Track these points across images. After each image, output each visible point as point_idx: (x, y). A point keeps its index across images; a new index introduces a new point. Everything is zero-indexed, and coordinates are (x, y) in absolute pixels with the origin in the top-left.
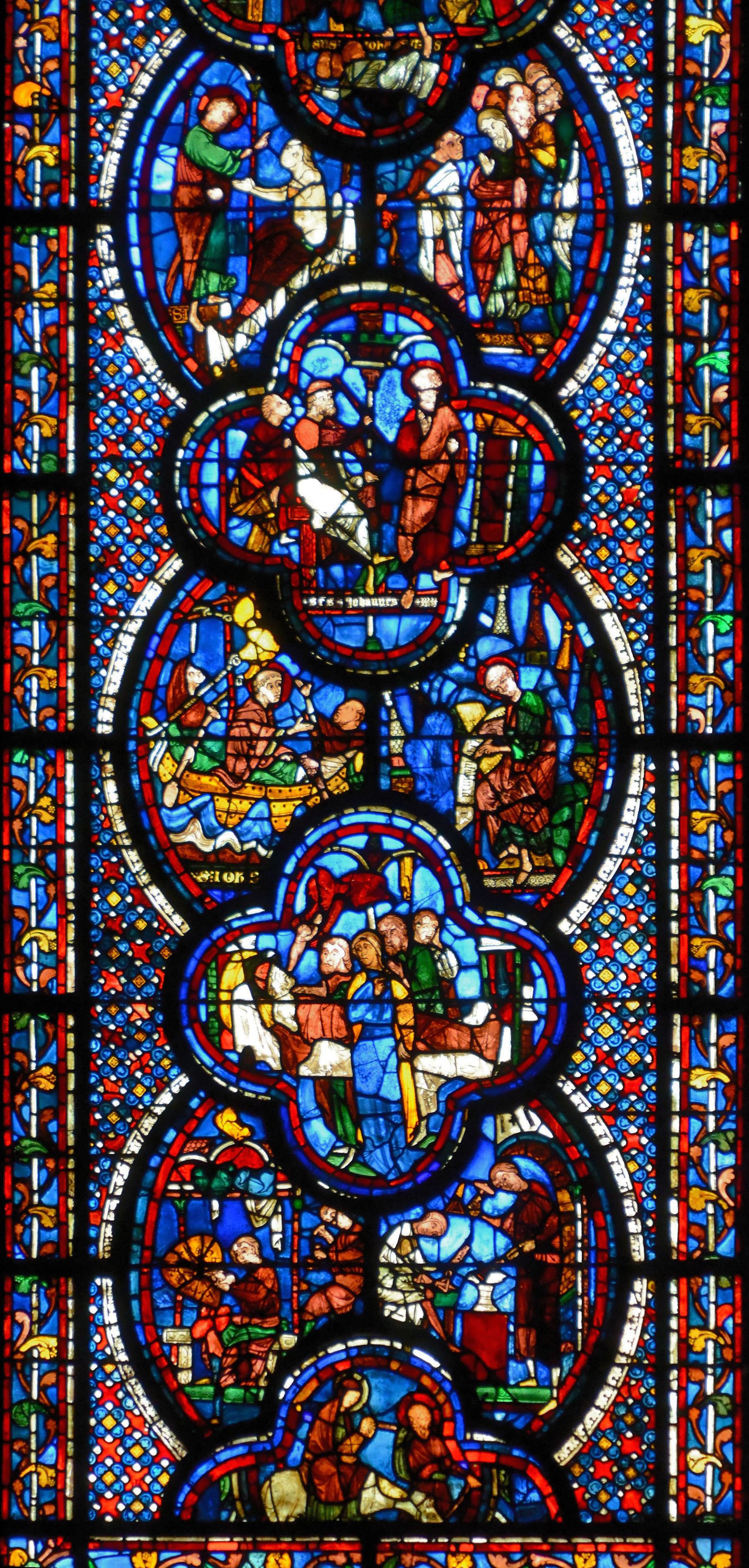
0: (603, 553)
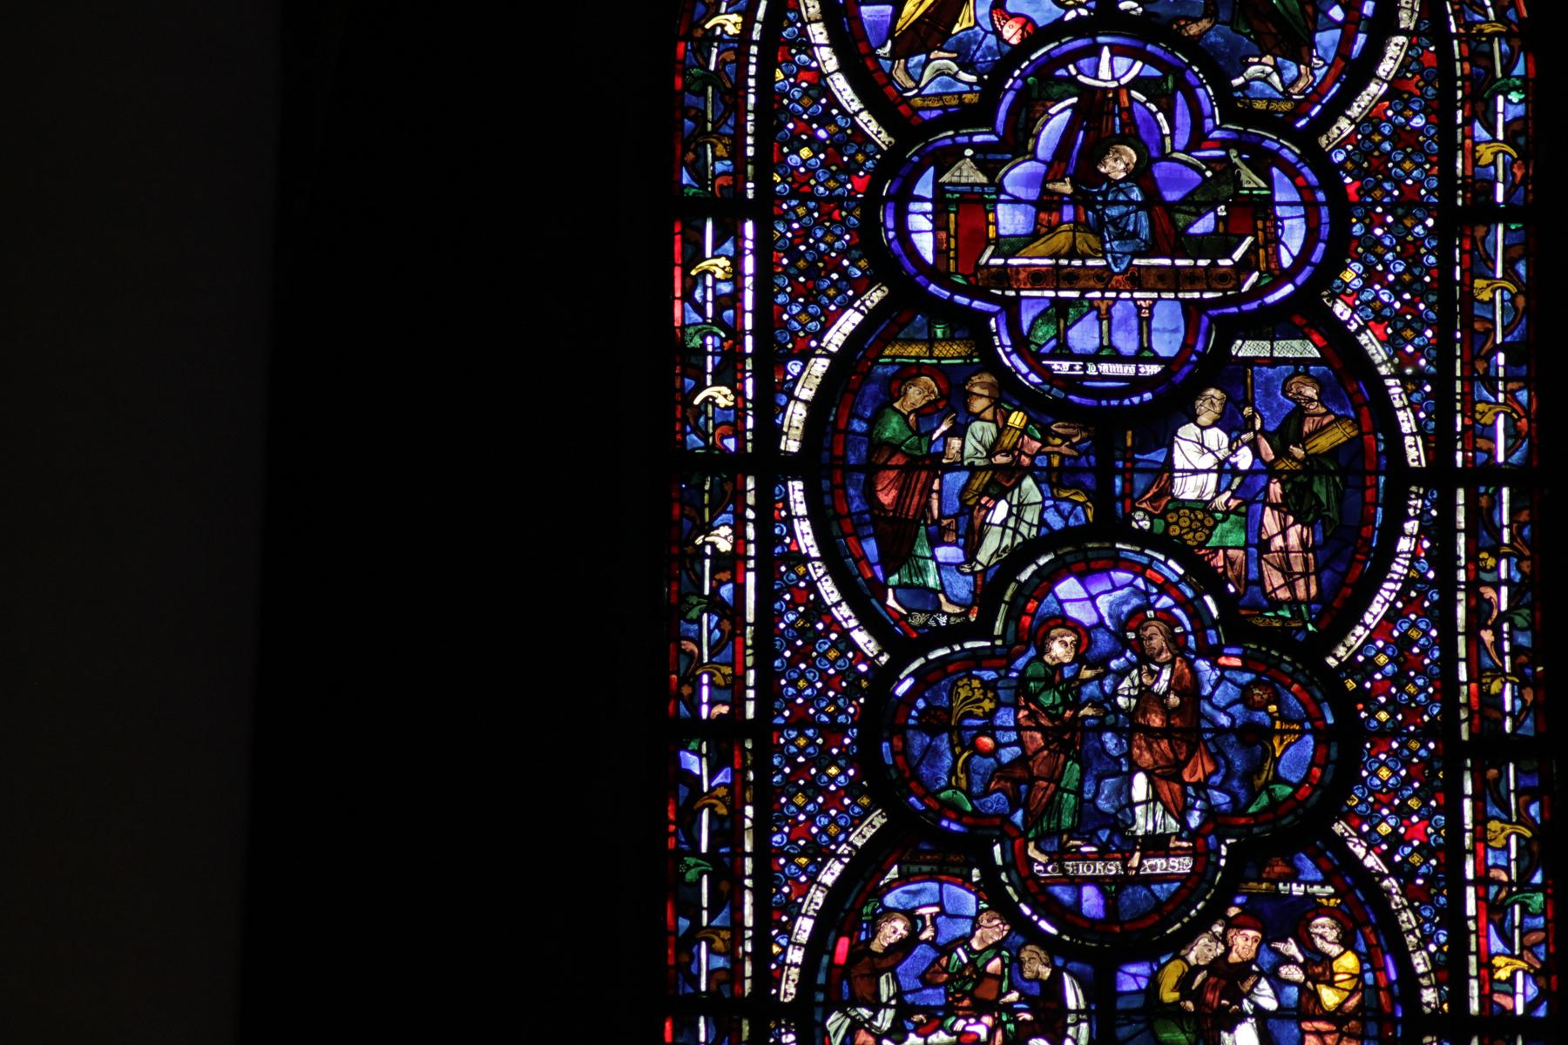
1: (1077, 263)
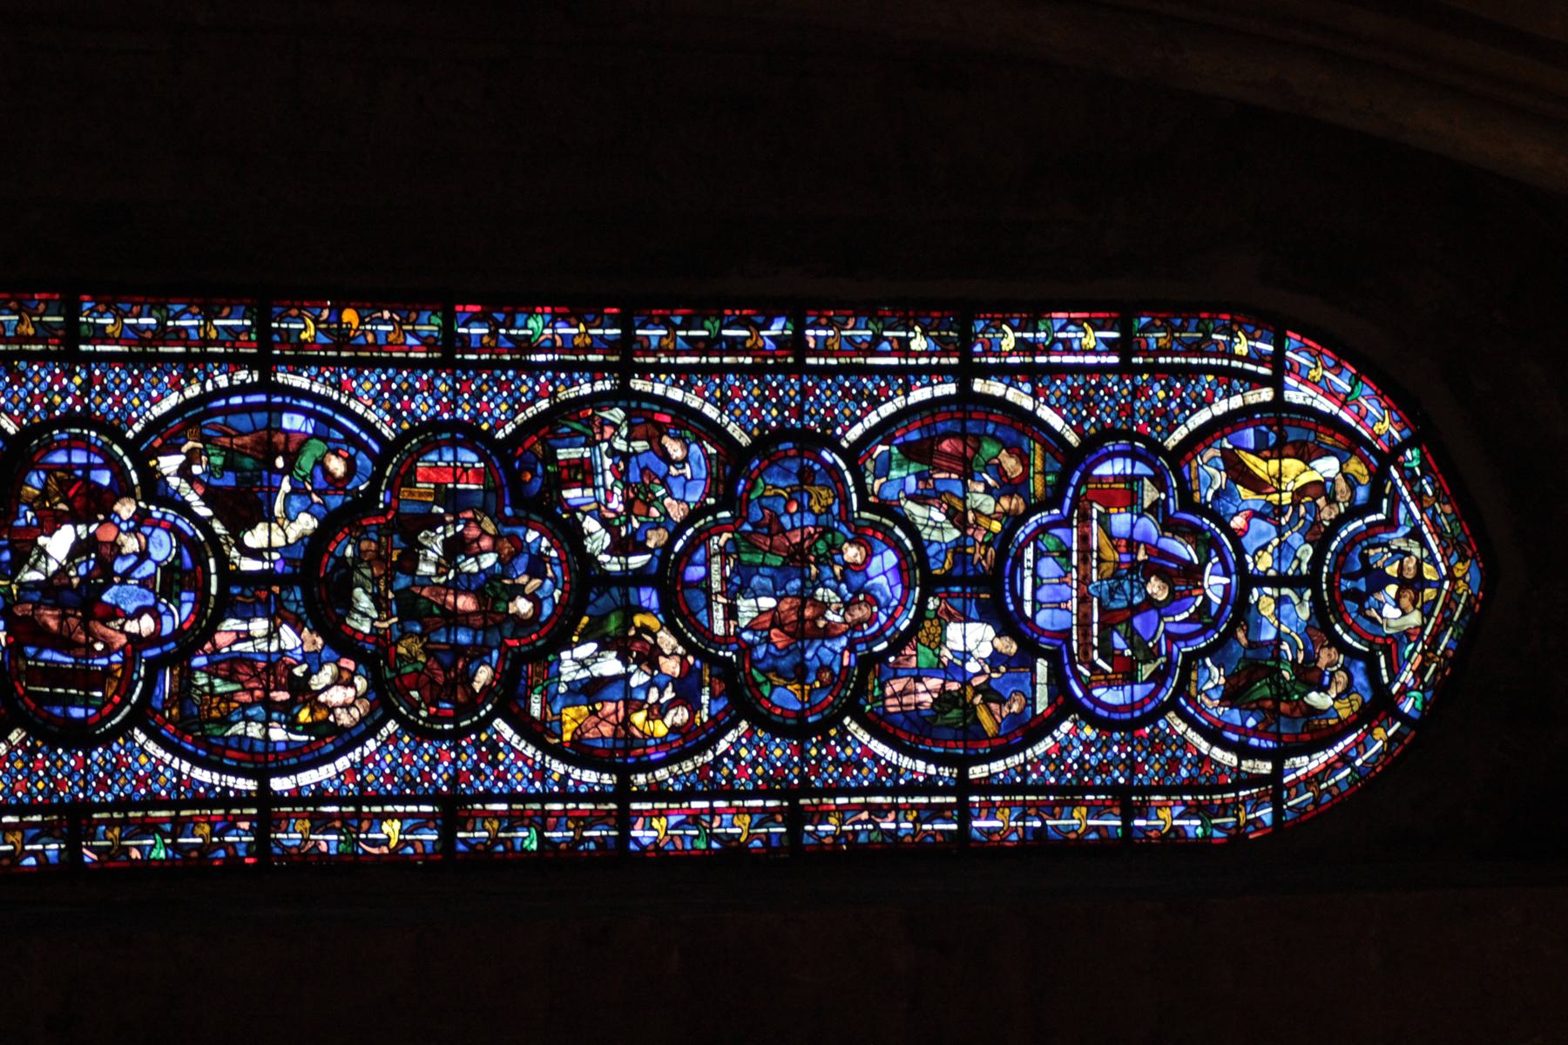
0: (19, 765)
1: (1094, 563)
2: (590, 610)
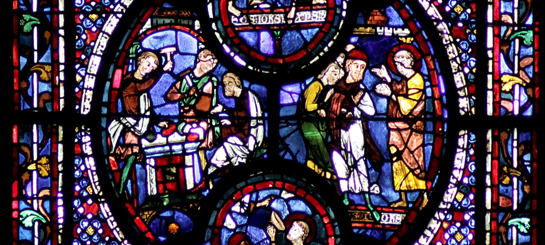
2: (301, 159)
